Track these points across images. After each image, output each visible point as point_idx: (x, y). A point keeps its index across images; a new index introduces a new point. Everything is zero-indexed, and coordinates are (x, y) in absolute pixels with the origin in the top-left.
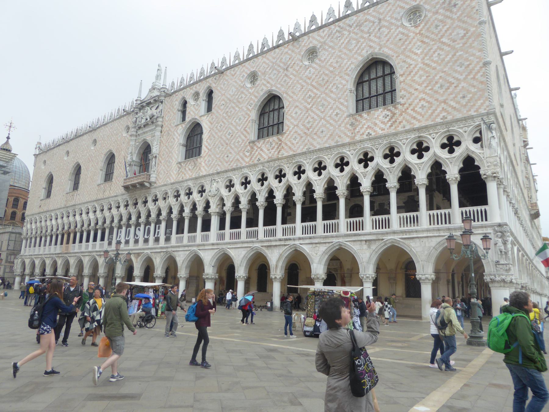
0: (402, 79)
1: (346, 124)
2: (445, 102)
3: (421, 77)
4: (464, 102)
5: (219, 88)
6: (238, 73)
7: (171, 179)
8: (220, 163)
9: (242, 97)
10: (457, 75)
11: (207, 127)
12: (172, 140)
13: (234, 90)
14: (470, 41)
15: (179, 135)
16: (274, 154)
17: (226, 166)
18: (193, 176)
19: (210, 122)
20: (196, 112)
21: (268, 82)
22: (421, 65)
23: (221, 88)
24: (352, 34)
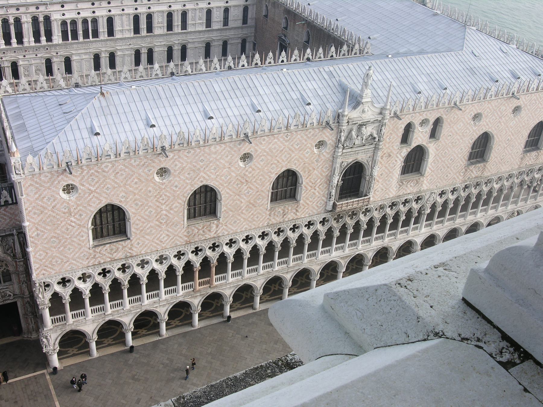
5: (449, 120)
6: (467, 111)
7: (390, 194)
8: (440, 181)
9: (466, 132)
11: (433, 153)
12: (394, 161)
13: (462, 125)
16: (479, 173)
18: (415, 191)
19: (437, 150)
21: (488, 125)
23: (451, 121)
24: (540, 105)
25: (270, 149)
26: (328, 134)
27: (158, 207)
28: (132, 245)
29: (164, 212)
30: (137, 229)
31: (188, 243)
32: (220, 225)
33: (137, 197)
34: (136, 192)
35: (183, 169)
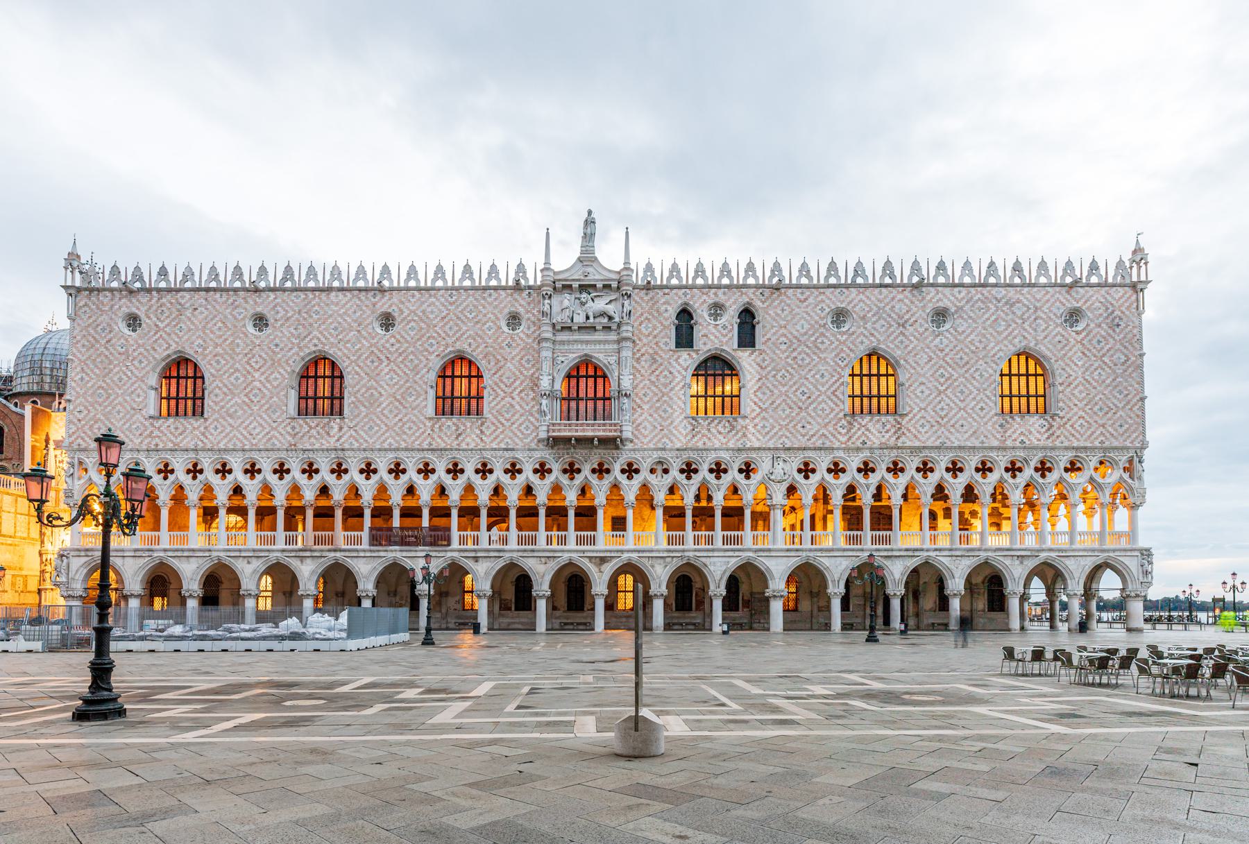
0: (1061, 388)
1: (995, 423)
2: (1103, 426)
3: (1081, 392)
4: (1121, 430)
6: (811, 300)
10: (1116, 402)
12: (666, 373)
13: (806, 326)
14: (1130, 370)
15: (686, 370)
17: (803, 442)
18: (731, 445)
20: (725, 340)
22: (1080, 379)
23: (777, 315)
25: (424, 312)
26: (523, 302)
27: (249, 372)
28: (206, 428)
29: (257, 384)
30: (216, 403)
31: (292, 448)
32: (345, 429)
33: (219, 350)
34: (219, 341)
35: (288, 319)
